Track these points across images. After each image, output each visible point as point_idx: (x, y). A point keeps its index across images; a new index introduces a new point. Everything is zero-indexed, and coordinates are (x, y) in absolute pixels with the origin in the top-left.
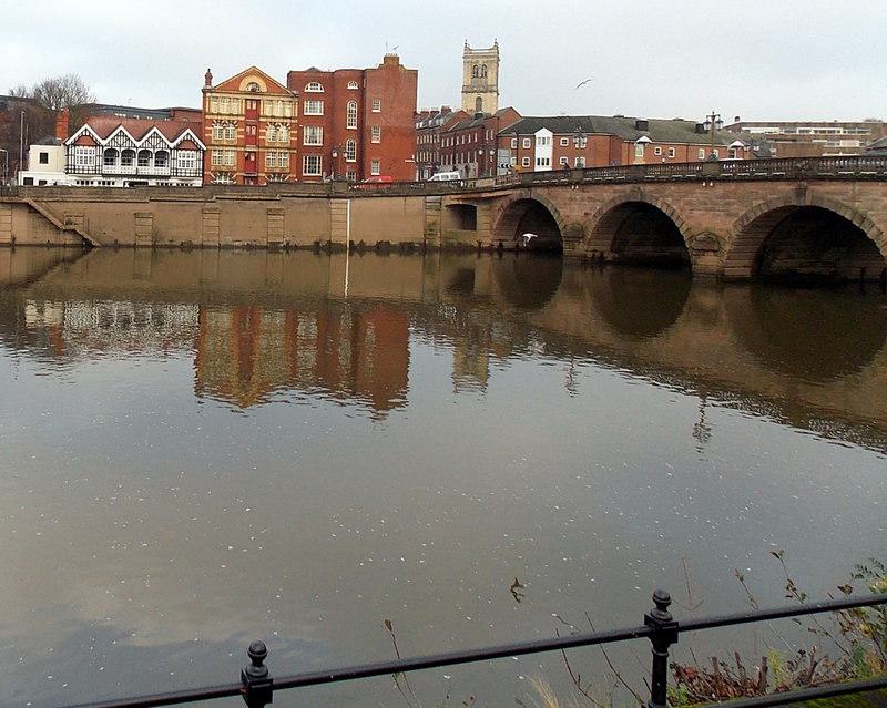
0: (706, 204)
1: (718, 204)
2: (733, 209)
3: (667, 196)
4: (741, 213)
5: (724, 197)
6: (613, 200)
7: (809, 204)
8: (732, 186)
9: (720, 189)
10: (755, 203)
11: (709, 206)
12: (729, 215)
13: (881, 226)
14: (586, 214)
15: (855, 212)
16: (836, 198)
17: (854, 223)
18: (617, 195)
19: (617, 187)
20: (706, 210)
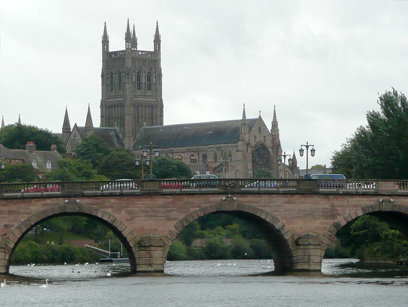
0: (148, 212)
1: (158, 212)
2: (175, 214)
3: (107, 207)
4: (182, 216)
5: (164, 206)
6: (45, 212)
7: (236, 209)
8: (170, 199)
9: (160, 201)
10: (192, 210)
11: (151, 214)
12: (169, 219)
13: (284, 222)
14: (6, 226)
15: (267, 214)
16: (254, 205)
17: (267, 220)
18: (46, 208)
19: (48, 201)
20: (149, 216)
